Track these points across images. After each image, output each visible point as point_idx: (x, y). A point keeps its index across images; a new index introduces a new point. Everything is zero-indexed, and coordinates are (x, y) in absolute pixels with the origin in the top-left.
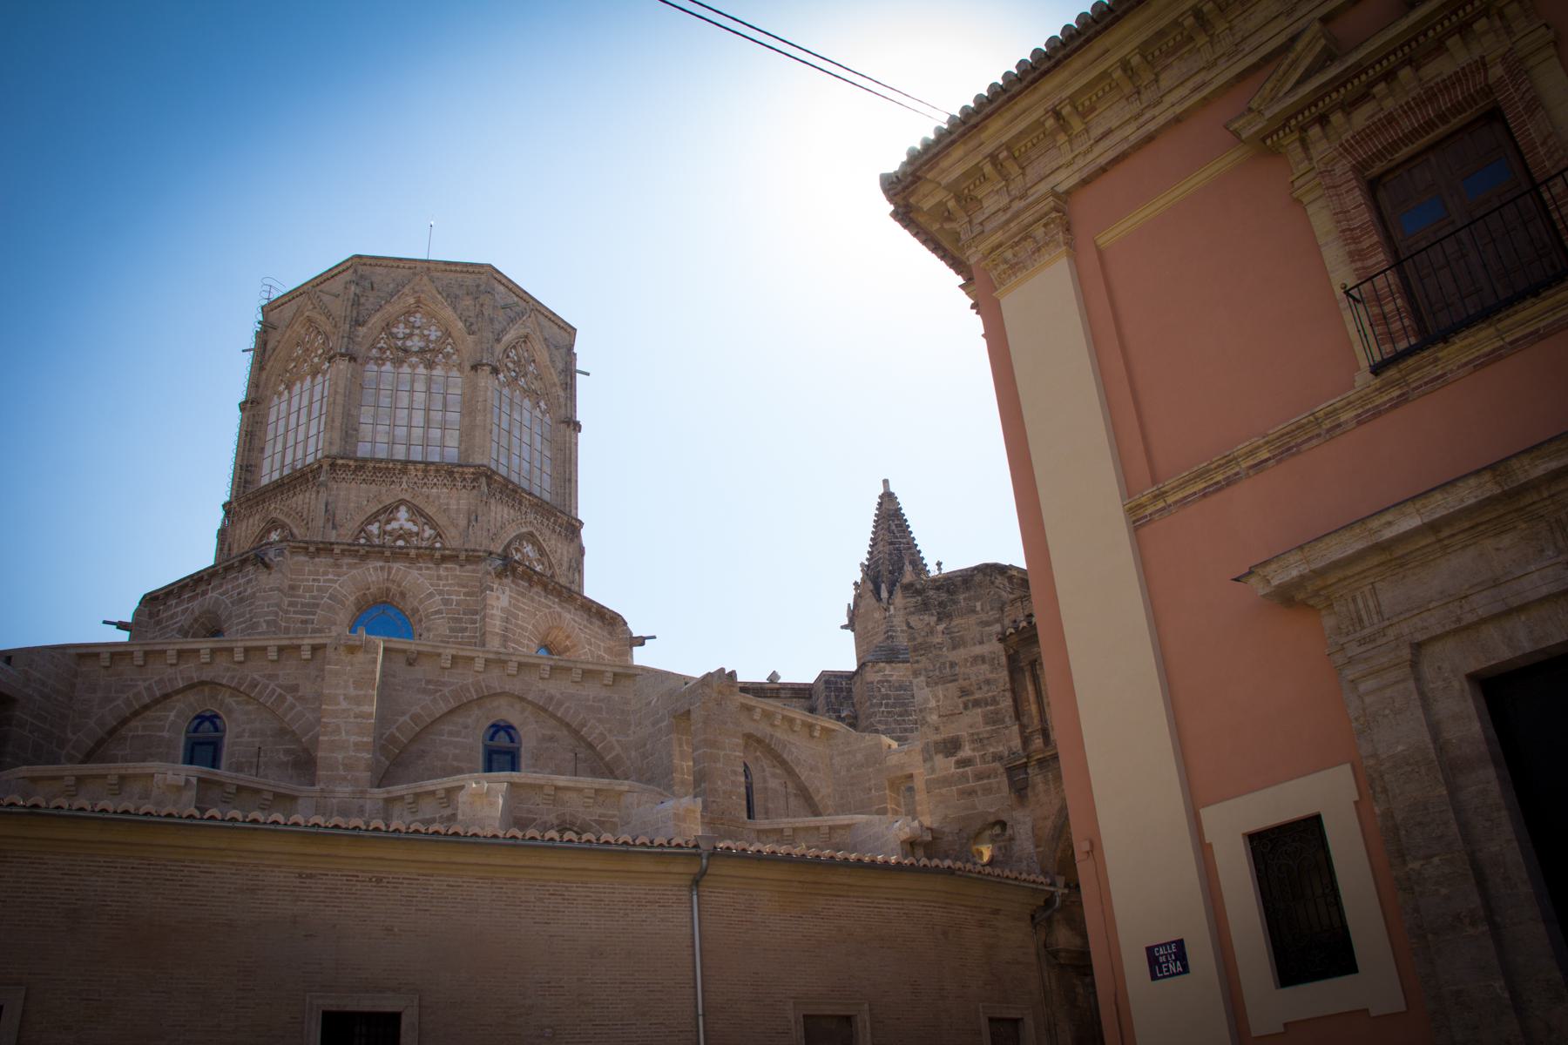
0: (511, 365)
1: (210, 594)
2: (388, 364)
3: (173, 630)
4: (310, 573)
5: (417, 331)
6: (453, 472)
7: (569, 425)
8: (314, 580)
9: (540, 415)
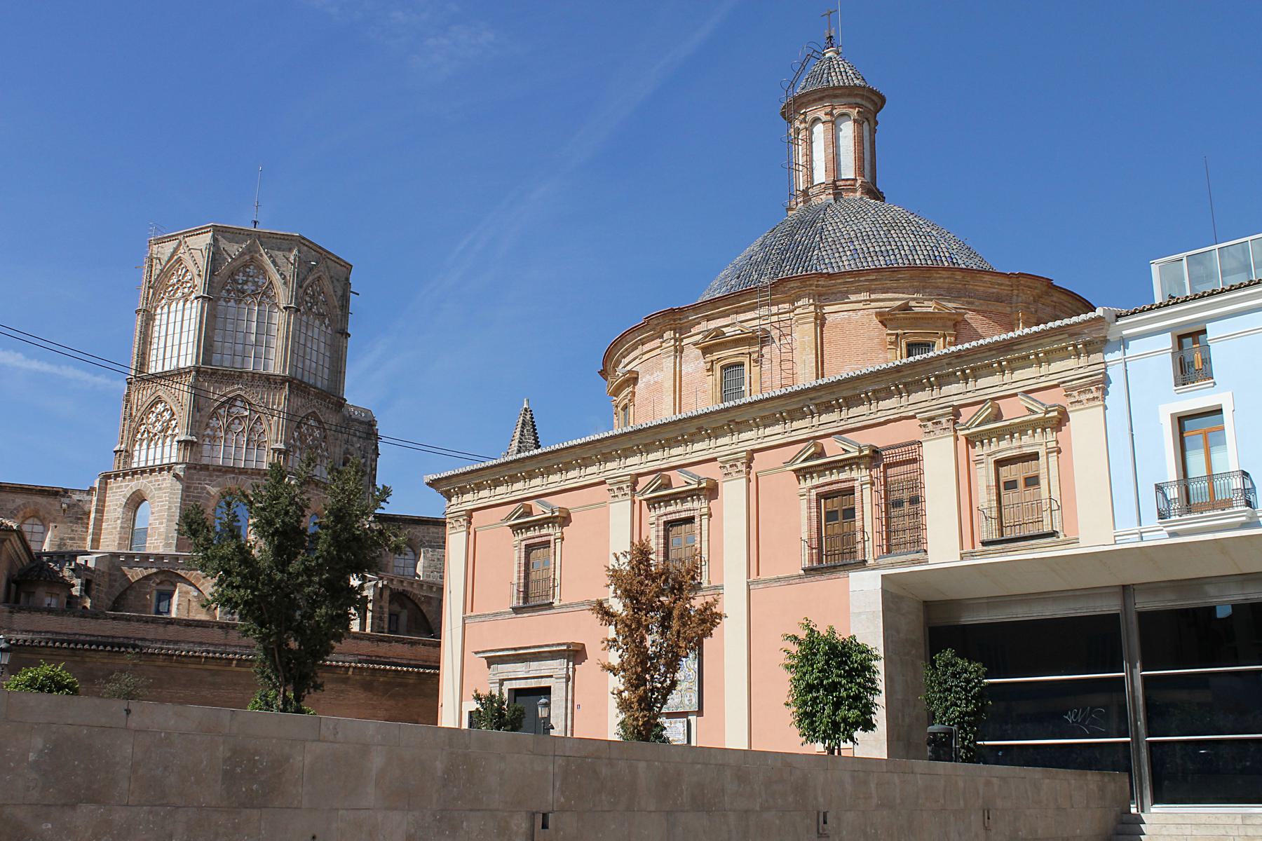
0: (308, 299)
1: (141, 481)
2: (232, 301)
3: (120, 495)
4: (197, 480)
5: (250, 279)
6: (269, 378)
7: (342, 336)
8: (199, 483)
9: (324, 329)
